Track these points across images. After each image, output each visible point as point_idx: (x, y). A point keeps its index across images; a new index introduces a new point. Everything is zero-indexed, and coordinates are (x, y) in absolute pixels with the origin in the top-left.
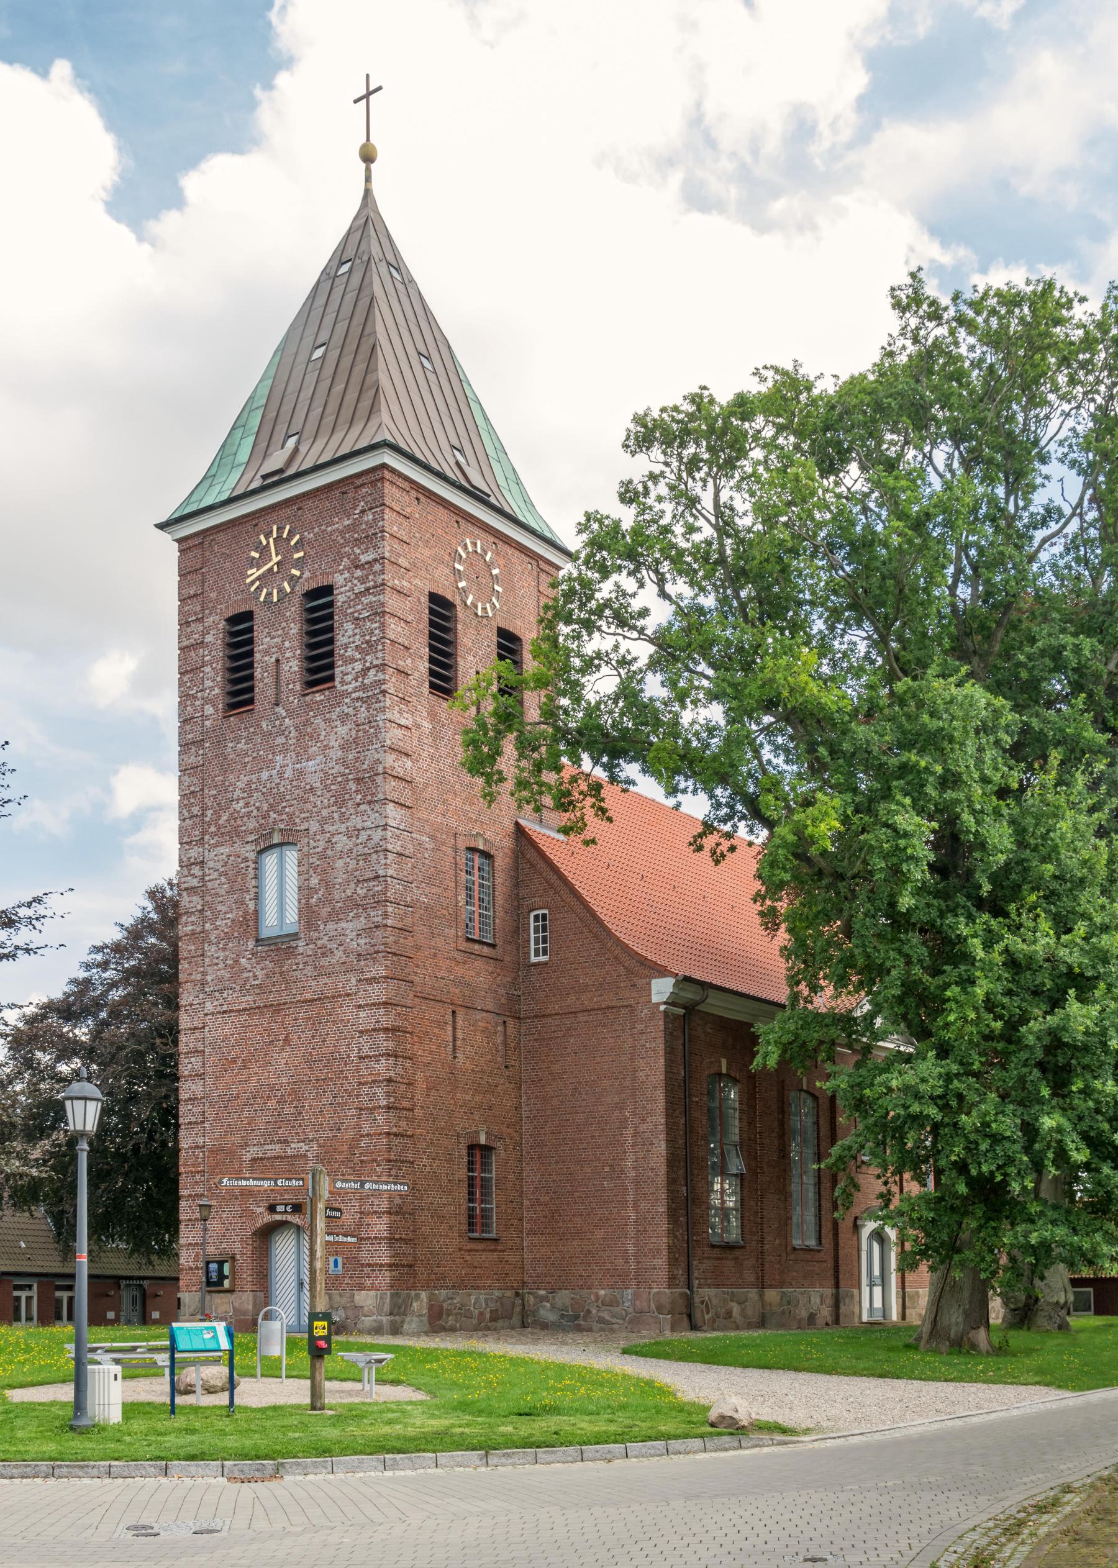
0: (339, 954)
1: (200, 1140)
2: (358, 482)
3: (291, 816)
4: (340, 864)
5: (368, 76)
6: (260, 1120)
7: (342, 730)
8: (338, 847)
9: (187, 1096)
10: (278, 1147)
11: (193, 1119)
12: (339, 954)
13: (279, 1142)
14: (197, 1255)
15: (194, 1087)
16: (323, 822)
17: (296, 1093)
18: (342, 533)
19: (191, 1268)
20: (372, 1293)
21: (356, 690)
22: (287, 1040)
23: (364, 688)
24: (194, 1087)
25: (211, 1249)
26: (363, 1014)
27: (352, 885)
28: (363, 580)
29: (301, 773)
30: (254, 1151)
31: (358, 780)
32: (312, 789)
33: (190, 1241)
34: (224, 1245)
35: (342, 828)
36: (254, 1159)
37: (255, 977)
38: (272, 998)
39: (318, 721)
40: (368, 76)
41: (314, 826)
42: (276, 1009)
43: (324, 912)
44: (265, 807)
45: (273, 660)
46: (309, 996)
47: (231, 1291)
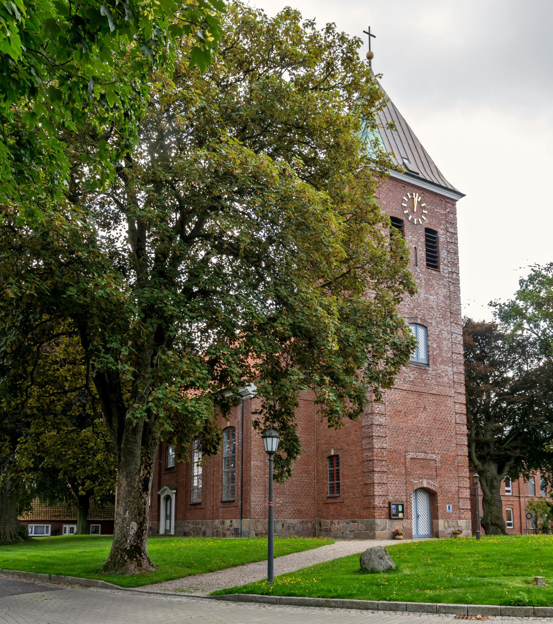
0: (446, 379)
1: (385, 446)
2: (448, 200)
3: (424, 315)
4: (445, 342)
5: (364, 32)
6: (413, 441)
7: (445, 291)
8: (444, 336)
9: (377, 423)
10: (423, 454)
11: (381, 435)
12: (446, 379)
13: (423, 452)
14: (384, 501)
15: (380, 419)
16: (438, 323)
17: (429, 432)
18: (441, 214)
19: (381, 507)
20: (464, 521)
21: (449, 277)
22: (424, 408)
23: (452, 278)
24: (380, 419)
25: (390, 498)
26: (457, 406)
27: (450, 353)
28: (451, 238)
29: (427, 299)
30: (411, 455)
31: (451, 313)
32: (432, 307)
33: (380, 493)
34: (397, 497)
35: (445, 329)
36: (411, 458)
37: (410, 377)
38: (418, 389)
39: (434, 281)
40: (364, 32)
41: (434, 324)
42: (420, 394)
43: (440, 359)
44: (412, 306)
45: (414, 246)
46: (435, 392)
47: (402, 519)
